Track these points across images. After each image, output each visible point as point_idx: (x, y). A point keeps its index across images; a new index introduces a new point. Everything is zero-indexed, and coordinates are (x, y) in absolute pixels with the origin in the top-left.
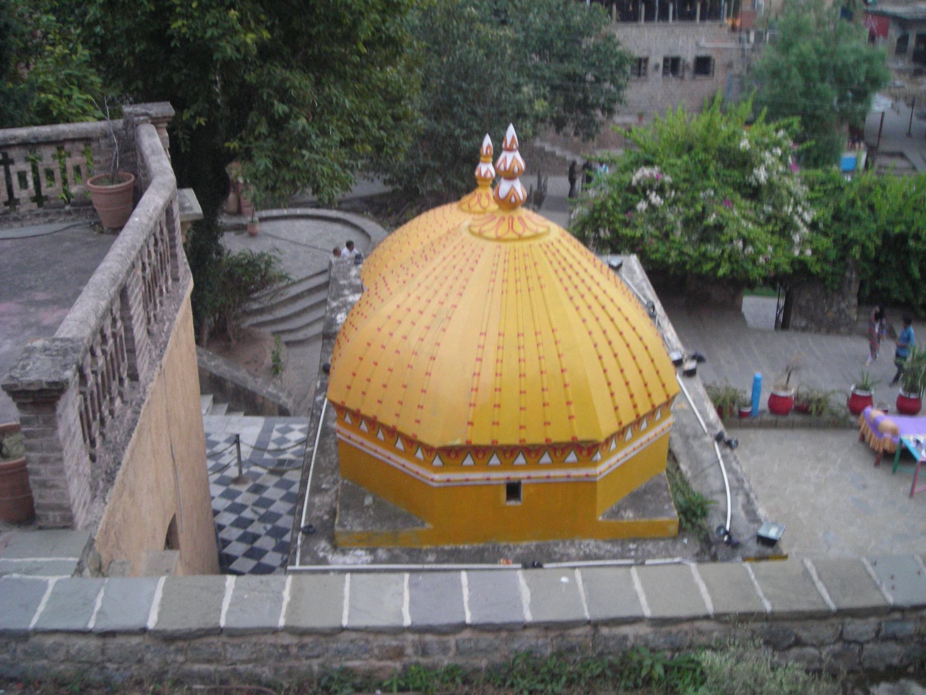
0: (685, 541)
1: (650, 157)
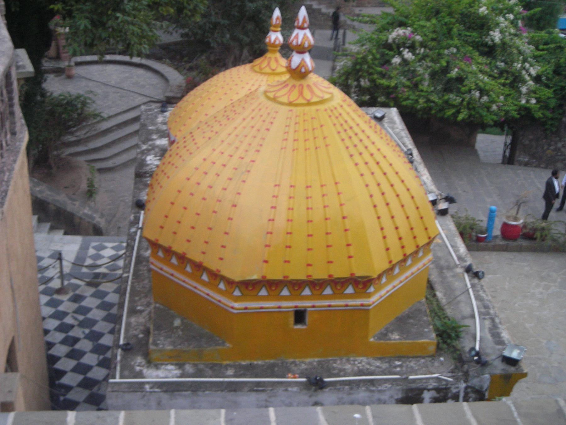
0: (442, 359)
1: (403, 19)
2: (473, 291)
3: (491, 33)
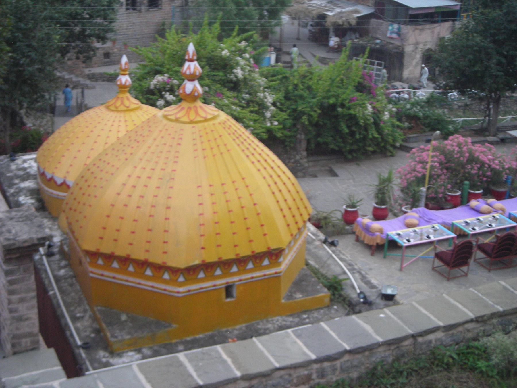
0: (335, 307)
3: (235, 71)
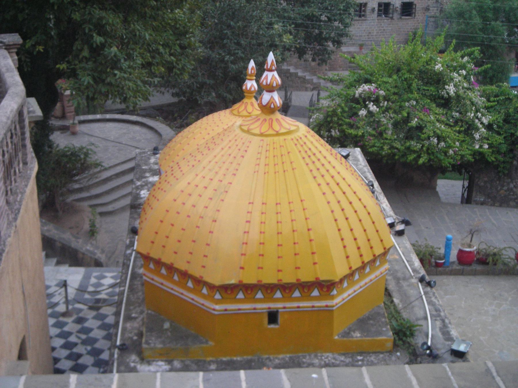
0: (398, 354)
1: (369, 77)
2: (426, 297)
